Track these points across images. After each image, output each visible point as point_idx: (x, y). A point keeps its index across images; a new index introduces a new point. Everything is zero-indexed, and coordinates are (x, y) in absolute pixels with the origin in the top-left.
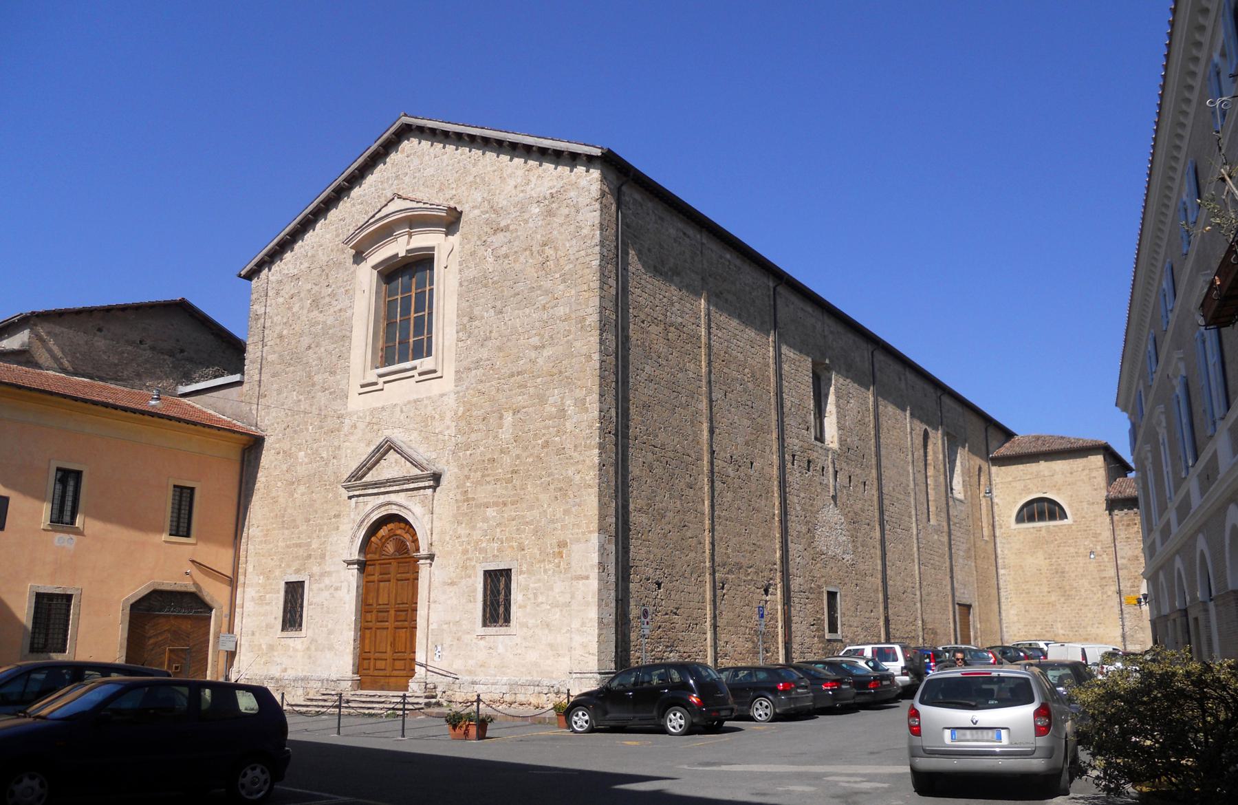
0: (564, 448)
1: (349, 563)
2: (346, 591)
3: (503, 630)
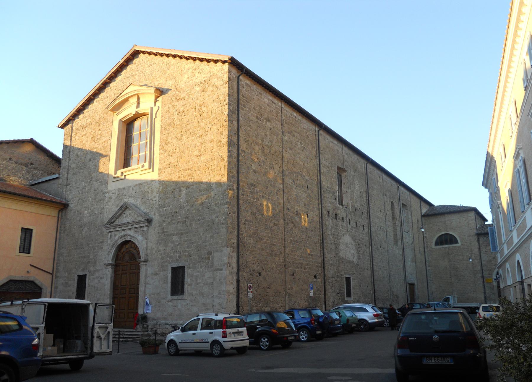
0: (210, 205)
1: (107, 265)
2: (106, 279)
3: (180, 297)
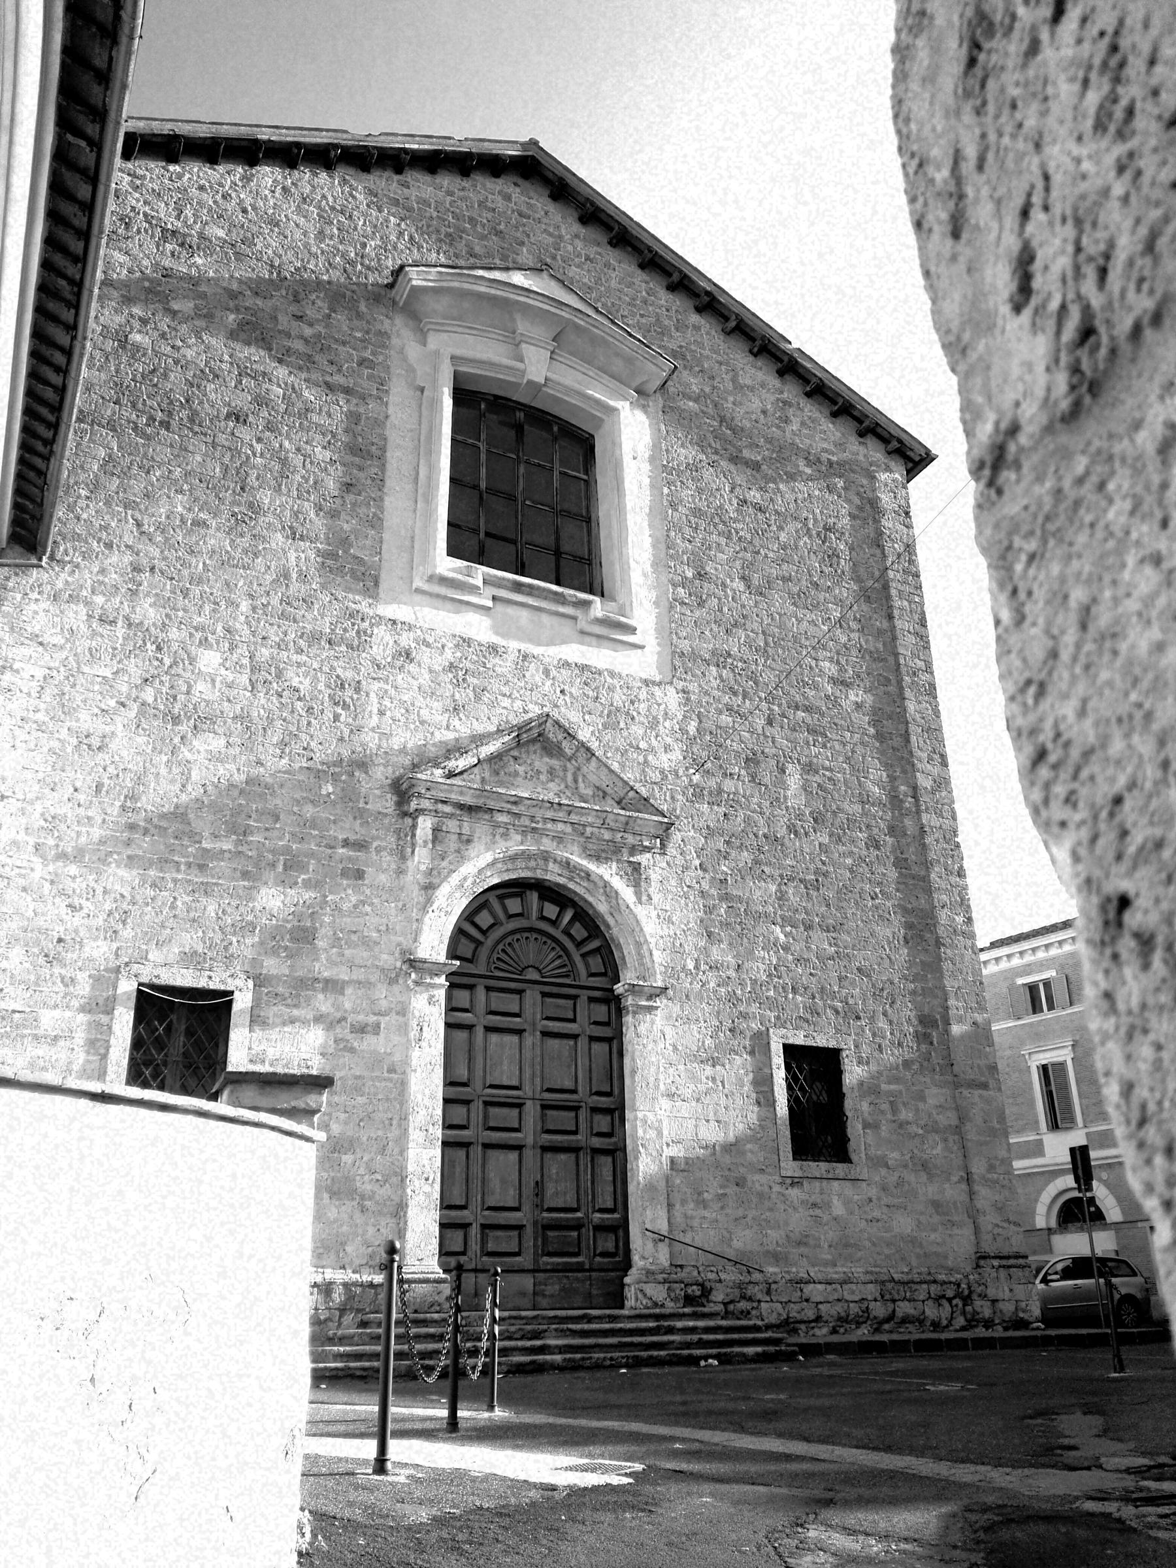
3: (840, 1169)
